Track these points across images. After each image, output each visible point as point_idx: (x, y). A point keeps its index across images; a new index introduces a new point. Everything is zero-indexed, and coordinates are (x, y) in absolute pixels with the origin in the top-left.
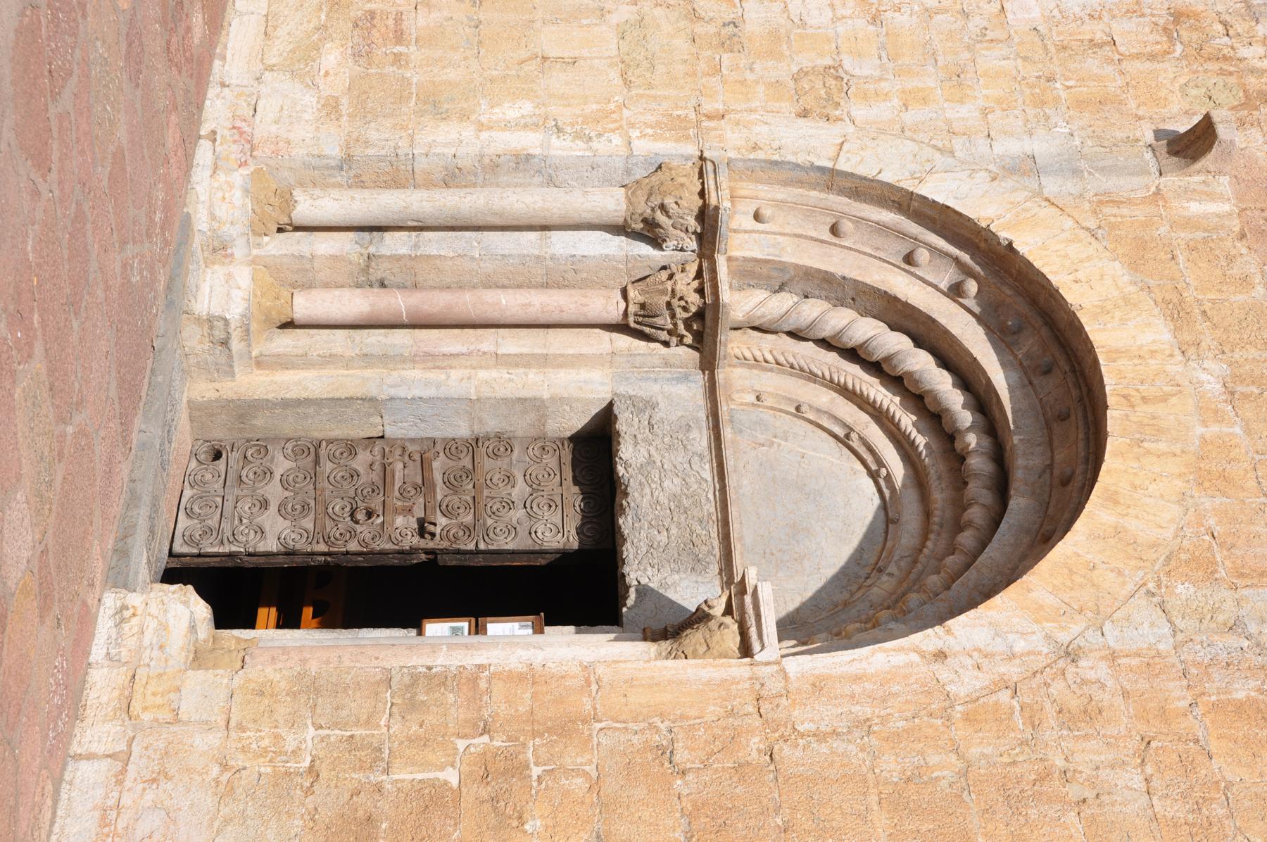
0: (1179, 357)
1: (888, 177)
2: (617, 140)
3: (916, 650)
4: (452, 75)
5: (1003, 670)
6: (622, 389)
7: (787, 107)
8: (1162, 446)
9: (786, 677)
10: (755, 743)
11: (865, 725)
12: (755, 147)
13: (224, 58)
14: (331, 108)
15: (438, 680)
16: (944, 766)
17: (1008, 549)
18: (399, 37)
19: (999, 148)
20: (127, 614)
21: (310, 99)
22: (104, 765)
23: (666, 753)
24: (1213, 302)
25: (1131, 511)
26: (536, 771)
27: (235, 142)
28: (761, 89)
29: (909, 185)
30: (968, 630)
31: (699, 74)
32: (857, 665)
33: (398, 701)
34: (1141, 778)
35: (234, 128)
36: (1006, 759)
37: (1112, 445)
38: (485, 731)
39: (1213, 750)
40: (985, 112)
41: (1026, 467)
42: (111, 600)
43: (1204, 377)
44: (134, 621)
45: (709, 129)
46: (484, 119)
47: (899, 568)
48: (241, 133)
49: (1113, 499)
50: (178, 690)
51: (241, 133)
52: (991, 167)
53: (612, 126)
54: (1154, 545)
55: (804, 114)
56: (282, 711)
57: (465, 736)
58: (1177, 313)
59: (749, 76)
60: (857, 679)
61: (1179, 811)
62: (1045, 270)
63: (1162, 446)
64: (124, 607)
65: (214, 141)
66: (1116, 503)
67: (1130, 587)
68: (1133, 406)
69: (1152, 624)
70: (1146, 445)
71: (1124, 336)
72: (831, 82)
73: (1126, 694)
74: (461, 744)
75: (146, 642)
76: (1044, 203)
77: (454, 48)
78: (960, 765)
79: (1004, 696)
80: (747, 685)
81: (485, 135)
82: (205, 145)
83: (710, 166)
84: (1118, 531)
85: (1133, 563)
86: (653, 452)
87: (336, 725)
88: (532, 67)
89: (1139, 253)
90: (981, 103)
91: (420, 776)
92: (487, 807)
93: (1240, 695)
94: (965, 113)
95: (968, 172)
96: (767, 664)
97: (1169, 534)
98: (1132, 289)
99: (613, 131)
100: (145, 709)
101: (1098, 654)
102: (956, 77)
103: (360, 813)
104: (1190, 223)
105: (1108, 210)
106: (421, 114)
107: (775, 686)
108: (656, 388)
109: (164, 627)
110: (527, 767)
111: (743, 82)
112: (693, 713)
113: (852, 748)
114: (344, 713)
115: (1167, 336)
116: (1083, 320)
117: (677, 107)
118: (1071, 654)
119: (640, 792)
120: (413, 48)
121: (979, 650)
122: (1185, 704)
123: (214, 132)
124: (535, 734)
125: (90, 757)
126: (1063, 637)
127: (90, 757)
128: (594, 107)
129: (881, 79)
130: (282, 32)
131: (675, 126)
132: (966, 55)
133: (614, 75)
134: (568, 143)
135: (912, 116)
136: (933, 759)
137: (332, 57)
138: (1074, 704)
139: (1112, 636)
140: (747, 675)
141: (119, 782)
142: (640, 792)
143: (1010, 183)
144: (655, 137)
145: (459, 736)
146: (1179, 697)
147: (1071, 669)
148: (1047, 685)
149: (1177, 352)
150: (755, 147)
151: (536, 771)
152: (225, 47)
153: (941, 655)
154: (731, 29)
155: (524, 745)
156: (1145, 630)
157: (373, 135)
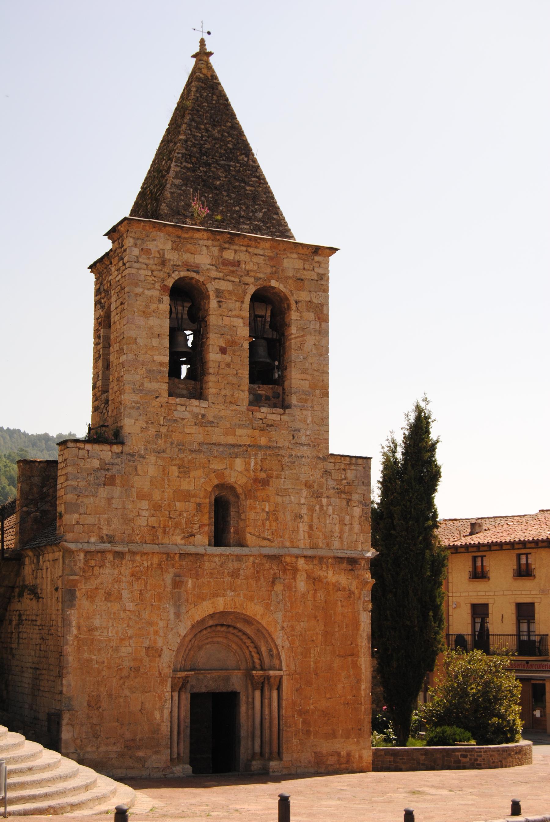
2: (167, 694)
6: (188, 691)
7: (157, 659)
8: (245, 605)
11: (294, 660)
12: (170, 666)
14: (156, 753)
16: (300, 649)
18: (134, 740)
19: (172, 619)
21: (154, 757)
28: (152, 664)
30: (279, 642)
40: (161, 619)
42: (271, 774)
43: (230, 594)
45: (164, 675)
46: (160, 721)
49: (255, 615)
51: (164, 769)
54: (264, 611)
55: (160, 656)
58: (216, 595)
59: (148, 666)
60: (286, 660)
61: (306, 619)
63: (245, 605)
71: (221, 604)
72: (150, 649)
73: (289, 621)
79: (289, 639)
81: (165, 721)
82: (167, 776)
84: (261, 615)
89: (201, 598)
94: (161, 624)
102: (150, 624)
104: (194, 588)
105: (190, 601)
106: (158, 734)
107: (288, 672)
109: (276, 765)
111: (150, 668)
117: (157, 682)
118: (283, 628)
126: (280, 628)
129: (150, 639)
130: (132, 765)
131: (163, 682)
132: (144, 621)
133: (147, 694)
134: (167, 704)
135: (162, 634)
136: (299, 651)
137: (141, 754)
138: (290, 629)
139: (280, 621)
143: (182, 618)
144: (166, 686)
146: (289, 614)
153: (283, 647)
154: (132, 669)
156: (279, 616)
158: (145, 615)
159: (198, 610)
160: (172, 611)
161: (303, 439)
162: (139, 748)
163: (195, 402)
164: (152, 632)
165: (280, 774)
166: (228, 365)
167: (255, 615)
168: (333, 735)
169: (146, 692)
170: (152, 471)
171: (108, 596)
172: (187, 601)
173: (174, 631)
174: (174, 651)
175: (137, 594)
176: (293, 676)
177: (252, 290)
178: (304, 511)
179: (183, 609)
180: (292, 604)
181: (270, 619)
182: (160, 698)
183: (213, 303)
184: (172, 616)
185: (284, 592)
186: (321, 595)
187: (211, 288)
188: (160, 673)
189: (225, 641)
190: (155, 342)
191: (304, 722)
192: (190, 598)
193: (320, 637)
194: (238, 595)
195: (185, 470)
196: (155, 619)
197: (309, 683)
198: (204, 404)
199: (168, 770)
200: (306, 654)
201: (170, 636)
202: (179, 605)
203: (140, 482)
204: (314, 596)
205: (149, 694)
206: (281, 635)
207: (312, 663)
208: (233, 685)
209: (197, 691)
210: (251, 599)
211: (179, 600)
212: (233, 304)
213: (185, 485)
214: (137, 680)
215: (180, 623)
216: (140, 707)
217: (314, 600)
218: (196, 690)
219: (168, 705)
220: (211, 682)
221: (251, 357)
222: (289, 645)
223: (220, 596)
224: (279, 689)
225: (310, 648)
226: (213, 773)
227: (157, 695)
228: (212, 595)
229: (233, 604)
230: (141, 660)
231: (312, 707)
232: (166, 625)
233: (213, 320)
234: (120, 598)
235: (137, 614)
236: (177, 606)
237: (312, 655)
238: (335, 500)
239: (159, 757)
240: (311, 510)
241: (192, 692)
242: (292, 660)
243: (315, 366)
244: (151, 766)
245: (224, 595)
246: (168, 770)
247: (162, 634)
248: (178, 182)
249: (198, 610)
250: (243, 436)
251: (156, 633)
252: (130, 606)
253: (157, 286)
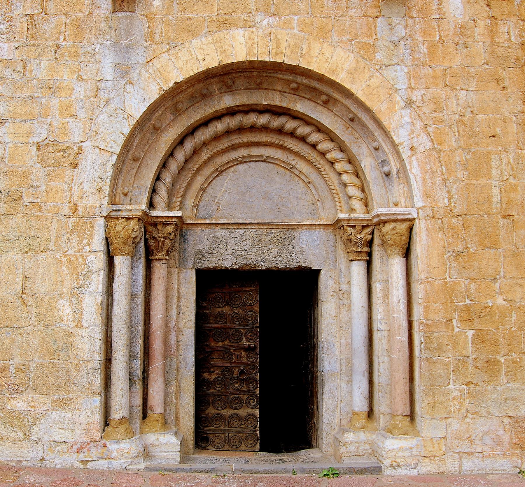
0: (254, 29)
1: (127, 131)
2: (92, 258)
3: (410, 157)
4: (35, 341)
5: (419, 128)
6: (190, 264)
7: (68, 172)
9: (425, 207)
10: (454, 221)
12: (100, 190)
13: (20, 461)
14: (61, 404)
15: (428, 338)
16: (459, 156)
17: (324, 116)
19: (110, 78)
20: (395, 464)
21: (55, 415)
22: (464, 461)
23: (457, 255)
24: (219, 9)
25: (340, 66)
26: (468, 302)
27: (89, 450)
28: (53, 184)
29: (133, 122)
30: (401, 137)
31: (40, 214)
32: (418, 180)
33: (437, 354)
34: (462, 91)
35: (78, 452)
36: (457, 134)
37: (303, 64)
38: (451, 321)
39: (448, 65)
40: (80, 79)
41: (281, 101)
42: (388, 472)
43: (265, 22)
44: (398, 460)
47: (293, 160)
48: (82, 448)
49: (334, 71)
50: (432, 439)
51: (82, 448)
52: (123, 82)
53: (80, 260)
54: (357, 62)
55: (75, 165)
56: (442, 398)
57: (453, 328)
59: (43, 188)
60: (424, 180)
61: (474, 83)
62: (196, 72)
63: (305, 47)
64: (392, 466)
65: (88, 461)
66: (336, 70)
67: (378, 74)
68: (282, 53)
69: (396, 71)
70: (304, 52)
71: (239, 47)
72: (50, 148)
74: (456, 330)
75: (409, 454)
76: (151, 64)
77: (12, 340)
78: (460, 150)
79: (430, 130)
80: (429, 222)
81: (85, 324)
83: (113, 214)
85: (366, 71)
86: (228, 253)
87: (448, 377)
88: (29, 300)
90: (74, 80)
91: (470, 345)
92: (483, 319)
93: (426, 51)
95: (126, 94)
96: (418, 213)
97: (352, 55)
98: (210, 39)
99: (85, 260)
100: (440, 450)
101: (410, 94)
102: (51, 89)
103: (485, 365)
105: (157, 38)
107: (429, 211)
108: (189, 249)
109: (402, 449)
110: (466, 305)
111: (48, 193)
112: (442, 243)
113: (455, 187)
114: (443, 374)
115: (241, 31)
116: (230, 61)
117: (66, 227)
118: (410, 103)
119: (476, 264)
120: (12, 362)
121: (410, 134)
122: (430, 69)
123: (82, 462)
124: (452, 302)
125: (460, 466)
126: (402, 104)
127: (460, 466)
128: (64, 268)
129: (50, 125)
131: (82, 228)
132: (35, 83)
133: (39, 257)
134: (93, 283)
135: (82, 114)
137: (19, 404)
138: (432, 106)
139: (402, 85)
140: (424, 221)
141: (472, 453)
142: (476, 264)
143: (134, 76)
144: (91, 238)
145: (453, 331)
147: (417, 104)
148: (424, 113)
149: (251, 29)
150: (100, 190)
151: (468, 302)
152: (11, 461)
153: (412, 149)
155: (457, 306)
156: (399, 75)
157: (85, 381)
158: (41, 70)
159: (177, 58)
160: (108, 61)
162: (16, 390)
164: (55, 110)
165: (414, 472)
167: (334, 71)
169: (37, 252)
172: (150, 36)
173: (114, 104)
174: (112, 153)
175: (21, 23)
176: (445, 220)
179: (139, 56)
180: (432, 48)
181: (375, 82)
182: (73, 266)
184: (108, 72)
185: (410, 21)
188: (75, 207)
189: (278, 154)
191: (480, 339)
192: (158, 31)
193: (514, 128)
194: (287, 25)
196: (65, 76)
197: (489, 241)
199: (93, 450)
200: (478, 167)
201: (103, 118)
202: (129, 47)
204: (492, 32)
205: (44, 255)
206: (407, 119)
207: (496, 192)
208: (302, 252)
209: (212, 265)
210: (322, 34)
211: (128, 36)
214: (13, 222)
215: (129, 87)
216: (20, 289)
217: (493, 43)
218: (209, 263)
220: (246, 246)
222: (429, 145)
223: (236, 26)
224: (407, 254)
225: (489, 153)
226: (261, 450)
227: (65, 259)
228: (215, 24)
229: (273, 45)
230: (26, 175)
231: (500, 301)
232: (93, 94)
235: (20, 68)
236: (124, 48)
237: (494, 172)
239: (69, 415)
241: (200, 266)
242: (438, 180)
244: (47, 438)
245: (248, 25)
246: (93, 450)
247: (82, 114)
249: (177, 58)
251: (67, 110)
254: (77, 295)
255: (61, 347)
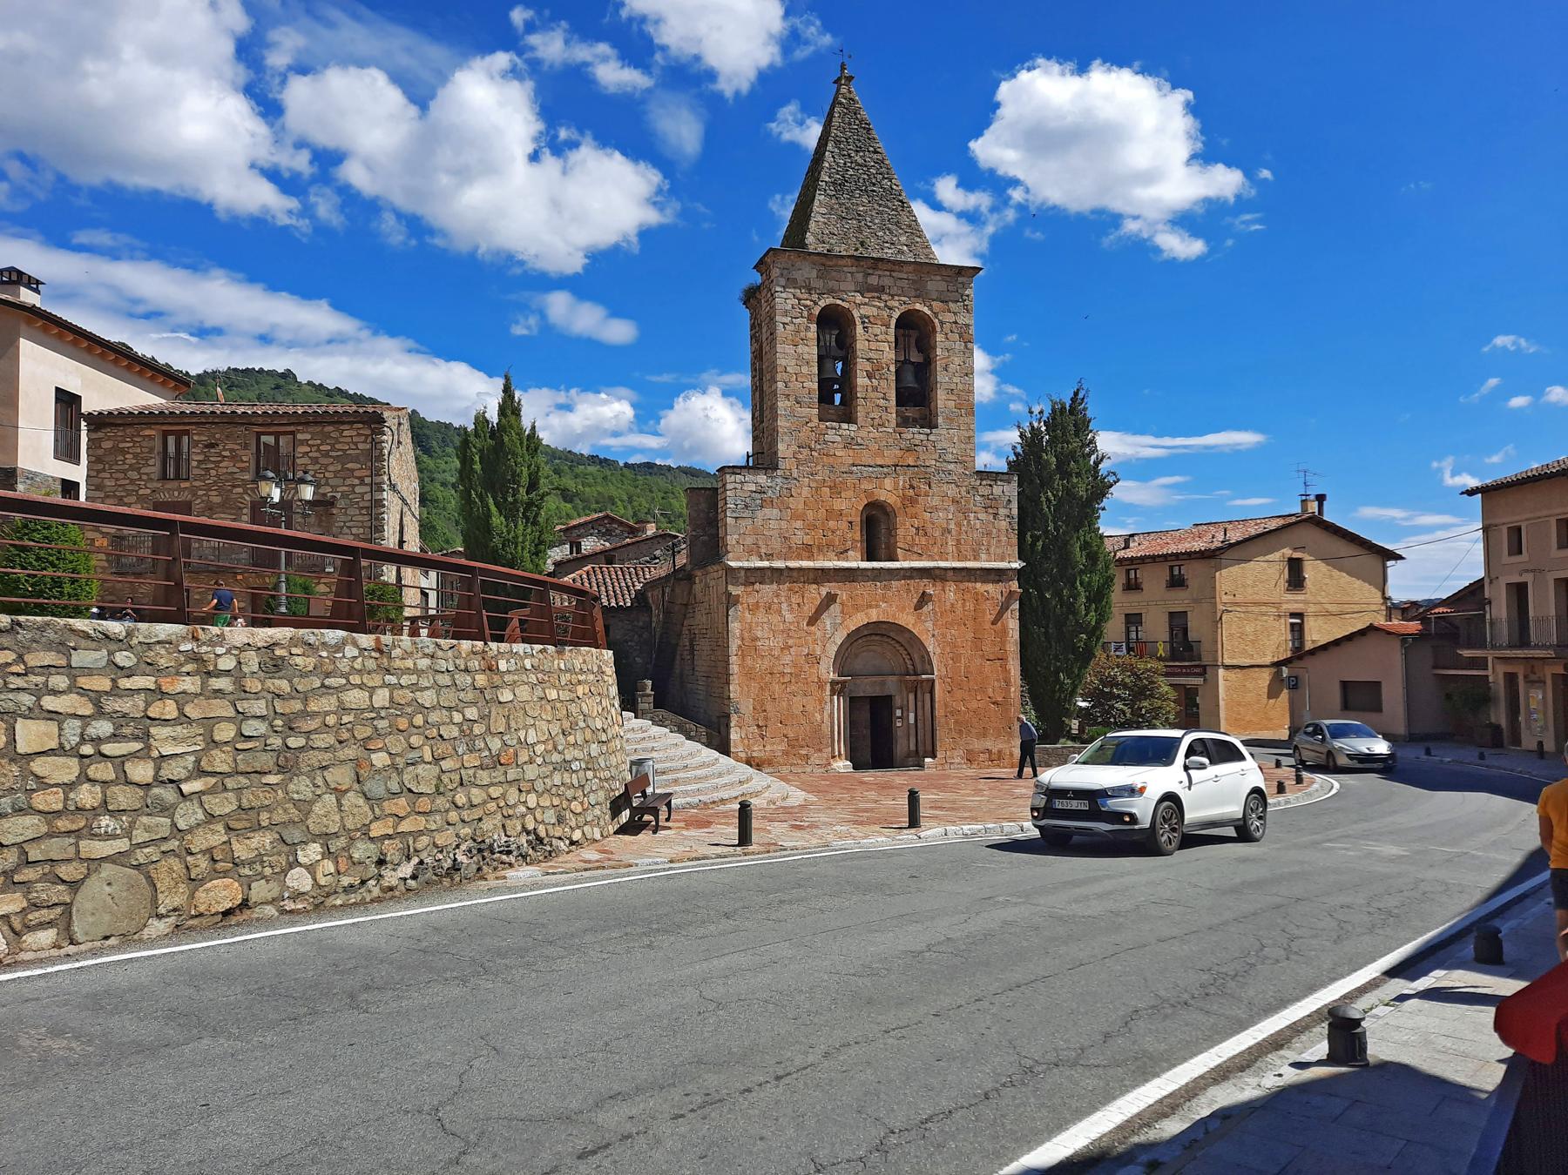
30: (930, 649)
71: (874, 615)
156: (929, 625)
161: (950, 457)
163: (845, 426)
166: (875, 389)
168: (985, 736)
170: (806, 491)
171: (768, 608)
177: (896, 315)
178: (952, 526)
183: (859, 329)
186: (970, 605)
187: (856, 314)
190: (805, 370)
191: (956, 722)
195: (836, 490)
198: (853, 427)
200: (956, 659)
203: (796, 504)
204: (964, 605)
212: (877, 329)
213: (839, 504)
219: (828, 707)
221: (898, 380)
224: (932, 692)
233: (861, 345)
234: (779, 612)
238: (982, 516)
240: (959, 525)
243: (960, 387)
245: (877, 606)
248: (823, 210)
250: (891, 455)
252: (789, 617)
253: (805, 314)
254: (822, 711)
255: (817, 729)
